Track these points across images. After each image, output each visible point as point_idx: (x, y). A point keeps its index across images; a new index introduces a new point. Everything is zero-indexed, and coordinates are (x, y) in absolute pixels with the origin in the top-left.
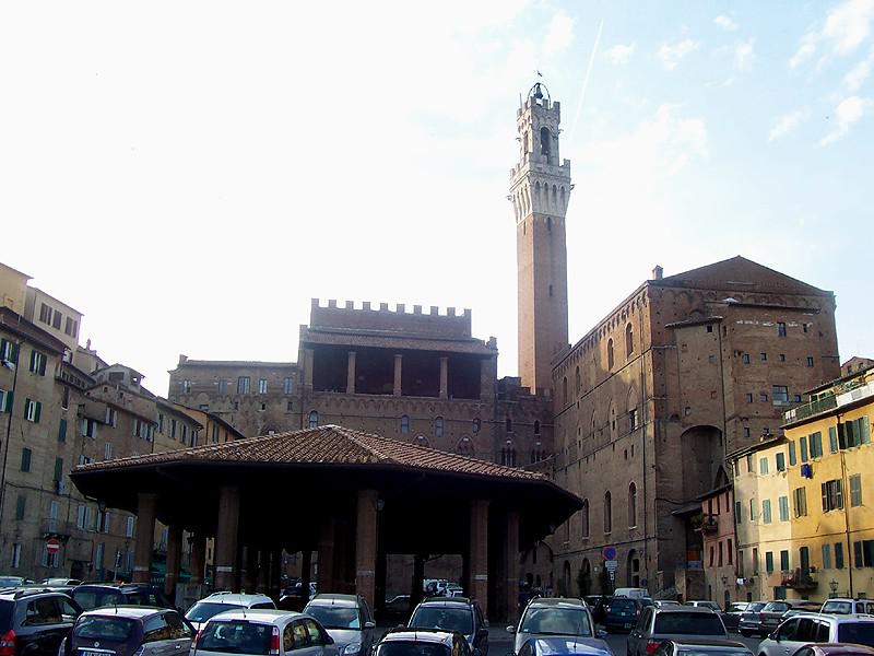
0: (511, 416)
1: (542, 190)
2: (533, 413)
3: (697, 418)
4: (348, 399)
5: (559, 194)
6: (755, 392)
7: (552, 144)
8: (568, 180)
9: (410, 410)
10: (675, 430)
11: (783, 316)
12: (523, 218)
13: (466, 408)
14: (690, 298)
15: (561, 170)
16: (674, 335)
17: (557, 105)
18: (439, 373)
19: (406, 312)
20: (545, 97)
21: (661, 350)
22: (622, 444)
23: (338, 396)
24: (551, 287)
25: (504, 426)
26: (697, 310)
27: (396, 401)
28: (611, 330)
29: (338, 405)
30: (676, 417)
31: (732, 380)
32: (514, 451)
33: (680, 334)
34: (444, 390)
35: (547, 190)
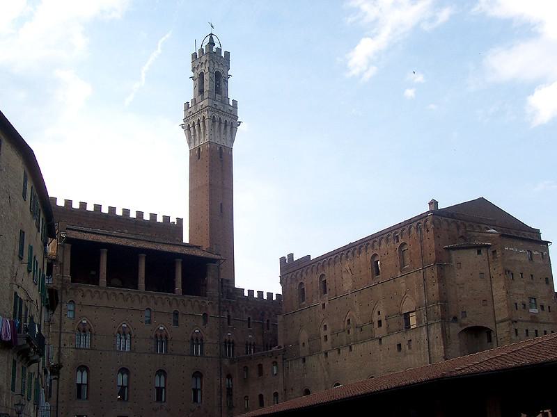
0: (231, 313)
1: (217, 124)
3: (472, 320)
4: (101, 291)
5: (229, 128)
6: (519, 301)
7: (223, 86)
10: (454, 329)
11: (530, 246)
14: (458, 227)
15: (231, 108)
16: (450, 255)
17: (227, 54)
20: (217, 45)
21: (442, 265)
23: (93, 287)
24: (221, 204)
26: (462, 237)
27: (141, 295)
32: (233, 343)
33: (455, 255)
34: (178, 288)
35: (220, 123)
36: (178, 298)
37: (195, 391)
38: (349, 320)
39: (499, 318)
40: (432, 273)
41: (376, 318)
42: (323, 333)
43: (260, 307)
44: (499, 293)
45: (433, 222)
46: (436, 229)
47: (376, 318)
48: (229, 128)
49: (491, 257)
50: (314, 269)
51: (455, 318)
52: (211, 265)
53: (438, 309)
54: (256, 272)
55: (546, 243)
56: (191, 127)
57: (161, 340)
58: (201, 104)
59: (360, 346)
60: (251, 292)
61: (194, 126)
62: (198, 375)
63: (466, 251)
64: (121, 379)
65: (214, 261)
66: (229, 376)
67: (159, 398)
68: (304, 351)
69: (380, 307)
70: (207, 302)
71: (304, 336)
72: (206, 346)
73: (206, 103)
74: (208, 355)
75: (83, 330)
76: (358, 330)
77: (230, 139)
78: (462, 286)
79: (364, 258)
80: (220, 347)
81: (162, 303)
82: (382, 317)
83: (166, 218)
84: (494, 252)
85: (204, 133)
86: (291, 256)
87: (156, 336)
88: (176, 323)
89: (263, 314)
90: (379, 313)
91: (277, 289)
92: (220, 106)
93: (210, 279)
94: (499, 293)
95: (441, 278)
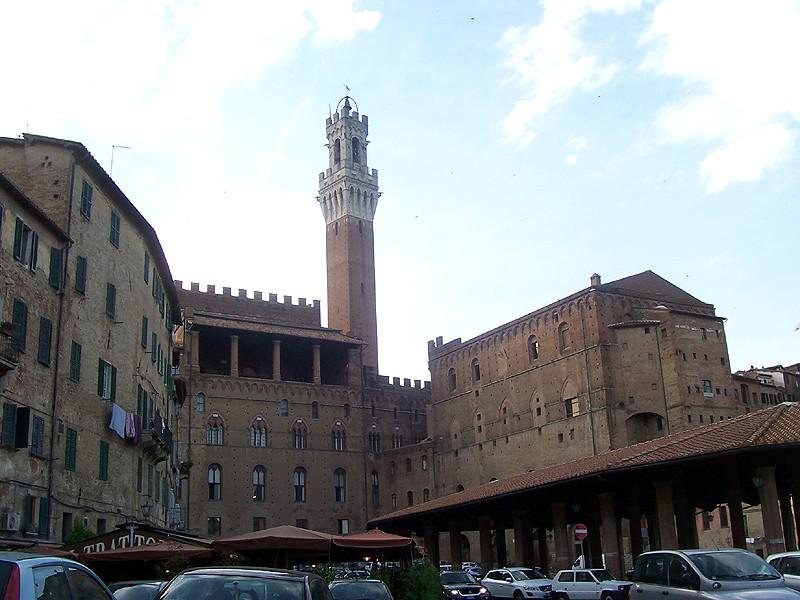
1: (356, 195)
3: (641, 406)
4: (233, 382)
6: (692, 385)
7: (361, 151)
9: (289, 394)
10: (621, 416)
11: (703, 323)
14: (623, 303)
15: (370, 178)
16: (615, 334)
17: (365, 118)
18: (312, 360)
19: (293, 303)
20: (354, 109)
21: (605, 346)
22: (556, 428)
25: (370, 411)
26: (627, 314)
28: (534, 326)
29: (224, 389)
31: (676, 374)
32: (378, 436)
33: (620, 334)
35: (359, 195)
37: (338, 490)
38: (505, 409)
39: (670, 404)
40: (596, 356)
41: (534, 406)
42: (476, 423)
43: (409, 398)
44: (670, 376)
45: (595, 299)
46: (600, 307)
47: (534, 406)
49: (660, 336)
50: (467, 354)
51: (622, 404)
53: (603, 394)
54: (402, 359)
55: (721, 319)
56: (328, 198)
57: (299, 433)
58: (338, 174)
59: (518, 438)
60: (396, 380)
61: (330, 199)
62: (340, 472)
63: (631, 330)
64: (257, 478)
65: (355, 346)
66: (374, 473)
67: (299, 498)
68: (456, 444)
69: (539, 394)
71: (456, 426)
72: (348, 440)
73: (343, 172)
74: (352, 450)
75: (214, 425)
76: (516, 418)
79: (520, 341)
81: (300, 394)
82: (541, 404)
83: (302, 301)
84: (664, 330)
85: (342, 204)
86: (440, 339)
87: (294, 430)
88: (316, 415)
89: (411, 404)
90: (538, 400)
91: (425, 376)
93: (351, 367)
94: (670, 376)
95: (606, 360)
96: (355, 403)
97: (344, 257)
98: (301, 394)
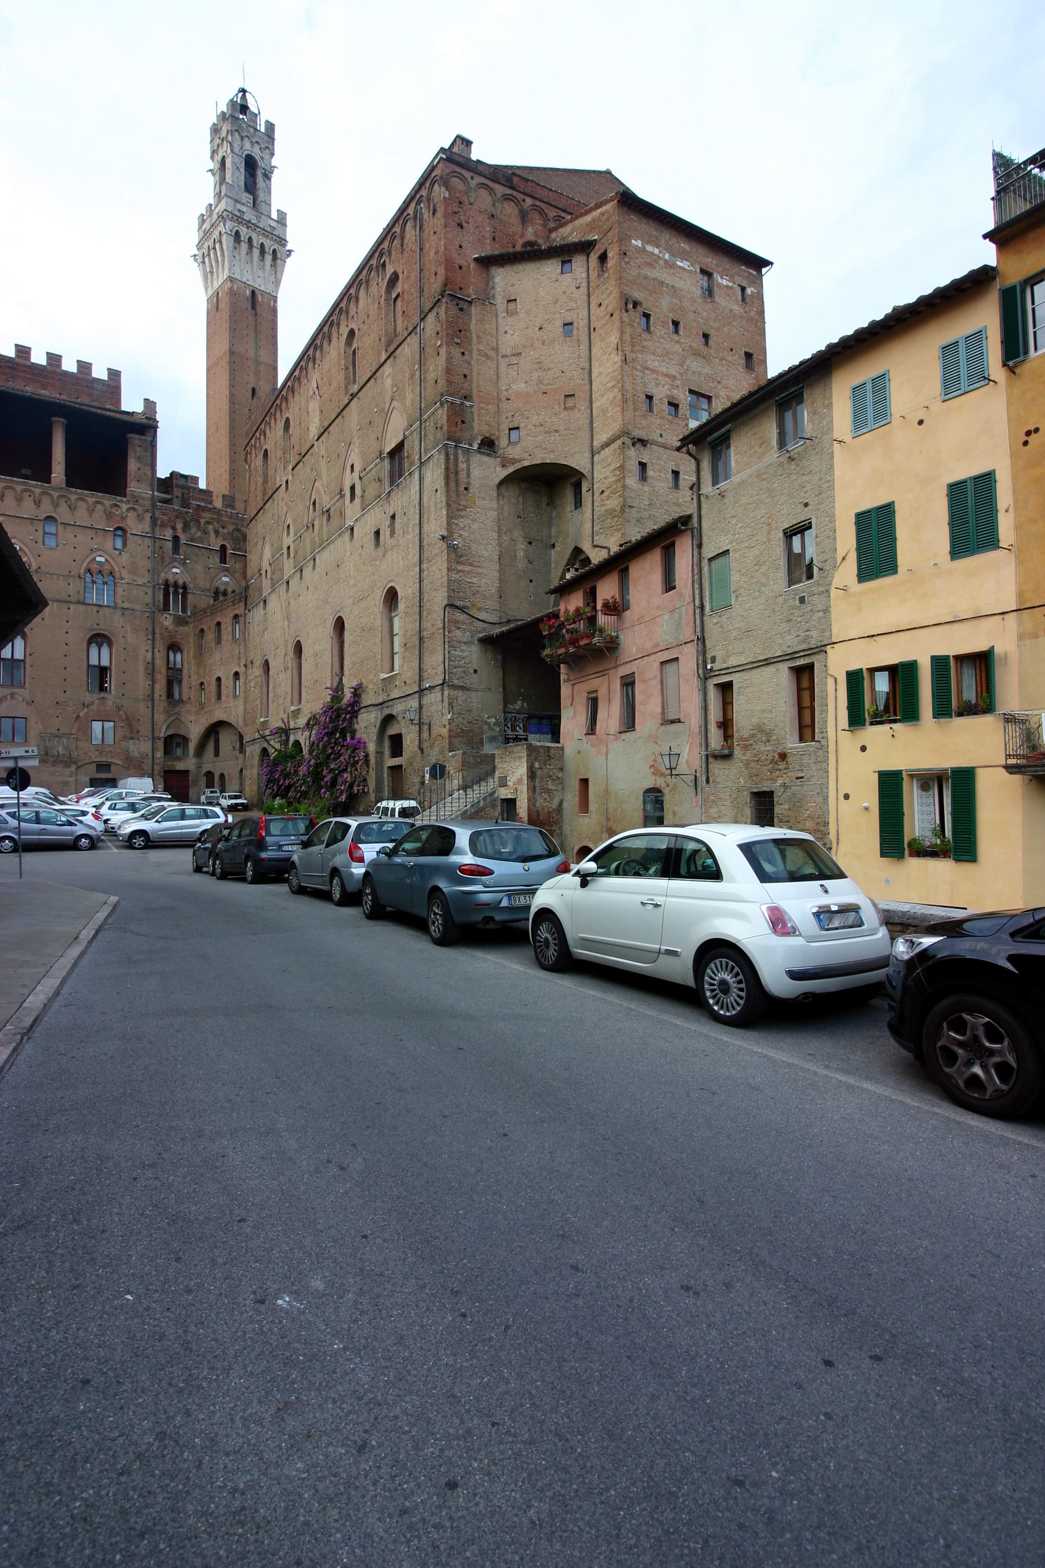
1: (244, 246)
2: (217, 532)
3: (532, 449)
5: (269, 258)
6: (661, 393)
8: (282, 241)
12: (216, 286)
13: (99, 507)
15: (274, 224)
16: (489, 279)
17: (270, 127)
25: (170, 545)
30: (488, 445)
32: (185, 587)
33: (502, 278)
36: (56, 494)
38: (314, 503)
48: (269, 258)
52: (134, 439)
53: (442, 415)
70: (125, 507)
74: (126, 605)
77: (272, 279)
78: (514, 360)
80: (154, 593)
83: (84, 367)
92: (249, 215)
93: (133, 465)
94: (606, 366)
96: (136, 526)
97: (223, 346)
98: (19, 500)
